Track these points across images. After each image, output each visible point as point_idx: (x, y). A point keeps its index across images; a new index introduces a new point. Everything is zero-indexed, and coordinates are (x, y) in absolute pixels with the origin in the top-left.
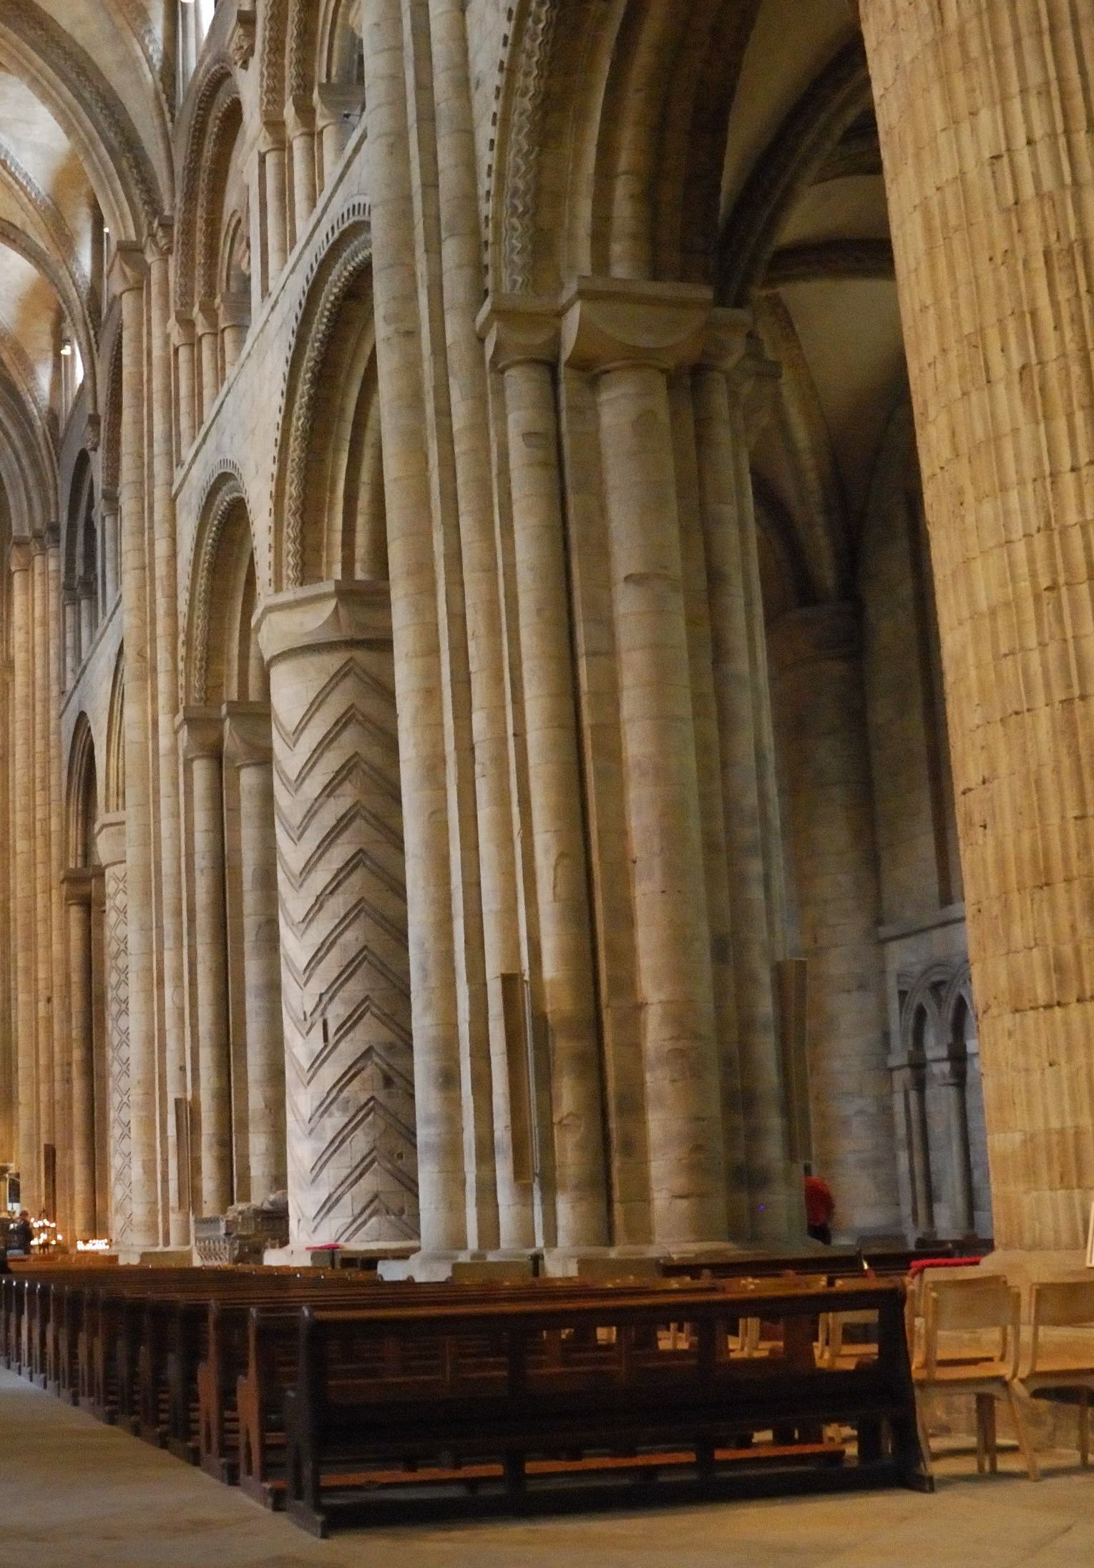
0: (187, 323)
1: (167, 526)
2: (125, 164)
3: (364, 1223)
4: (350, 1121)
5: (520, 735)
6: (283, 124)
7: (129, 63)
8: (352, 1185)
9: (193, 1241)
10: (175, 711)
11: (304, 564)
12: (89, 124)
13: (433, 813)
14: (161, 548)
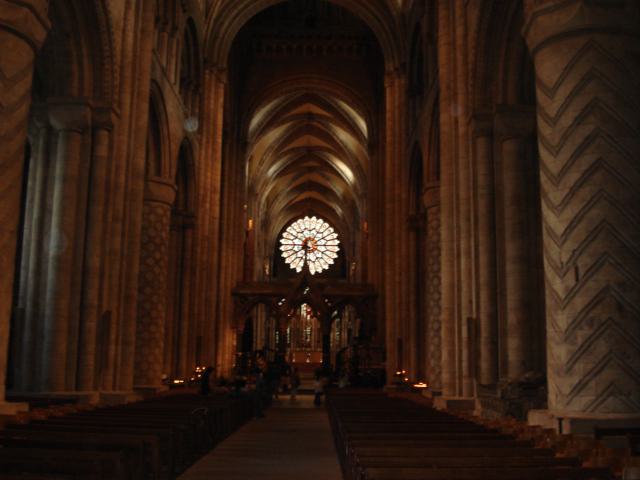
4: (594, 333)
8: (596, 375)
9: (475, 395)
14: (460, 31)
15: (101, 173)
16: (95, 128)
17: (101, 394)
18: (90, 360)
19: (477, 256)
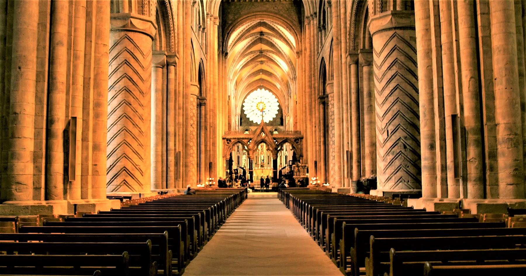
1: (344, 5)
3: (398, 184)
5: (457, 41)
10: (346, 52)
11: (382, 7)
13: (428, 67)
14: (342, 11)
15: (172, 87)
16: (168, 65)
17: (178, 190)
18: (172, 174)
19: (351, 122)
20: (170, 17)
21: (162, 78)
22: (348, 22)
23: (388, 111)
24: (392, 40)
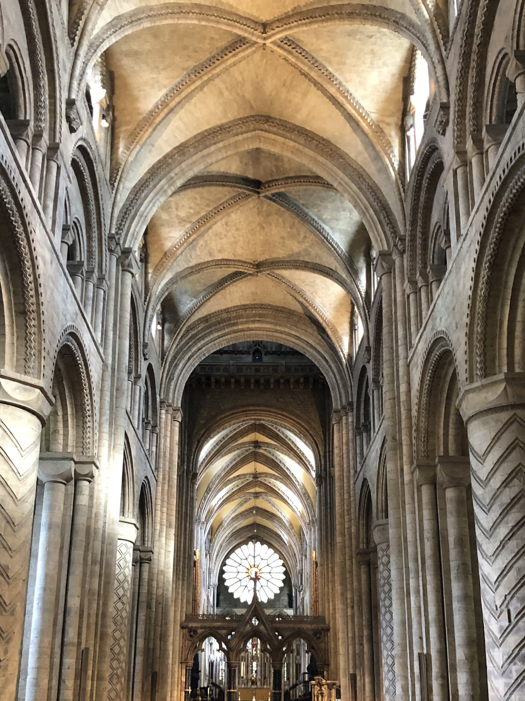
0: (413, 283)
1: (405, 378)
2: (382, 217)
6: (466, 152)
7: (384, 169)
10: (412, 463)
11: (486, 367)
12: (365, 200)
14: (403, 388)
19: (425, 594)
20: (86, 392)
21: (64, 504)
22: (415, 408)
23: (507, 570)
24: (508, 431)
